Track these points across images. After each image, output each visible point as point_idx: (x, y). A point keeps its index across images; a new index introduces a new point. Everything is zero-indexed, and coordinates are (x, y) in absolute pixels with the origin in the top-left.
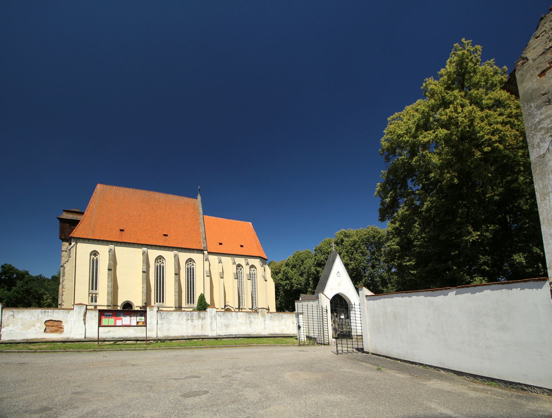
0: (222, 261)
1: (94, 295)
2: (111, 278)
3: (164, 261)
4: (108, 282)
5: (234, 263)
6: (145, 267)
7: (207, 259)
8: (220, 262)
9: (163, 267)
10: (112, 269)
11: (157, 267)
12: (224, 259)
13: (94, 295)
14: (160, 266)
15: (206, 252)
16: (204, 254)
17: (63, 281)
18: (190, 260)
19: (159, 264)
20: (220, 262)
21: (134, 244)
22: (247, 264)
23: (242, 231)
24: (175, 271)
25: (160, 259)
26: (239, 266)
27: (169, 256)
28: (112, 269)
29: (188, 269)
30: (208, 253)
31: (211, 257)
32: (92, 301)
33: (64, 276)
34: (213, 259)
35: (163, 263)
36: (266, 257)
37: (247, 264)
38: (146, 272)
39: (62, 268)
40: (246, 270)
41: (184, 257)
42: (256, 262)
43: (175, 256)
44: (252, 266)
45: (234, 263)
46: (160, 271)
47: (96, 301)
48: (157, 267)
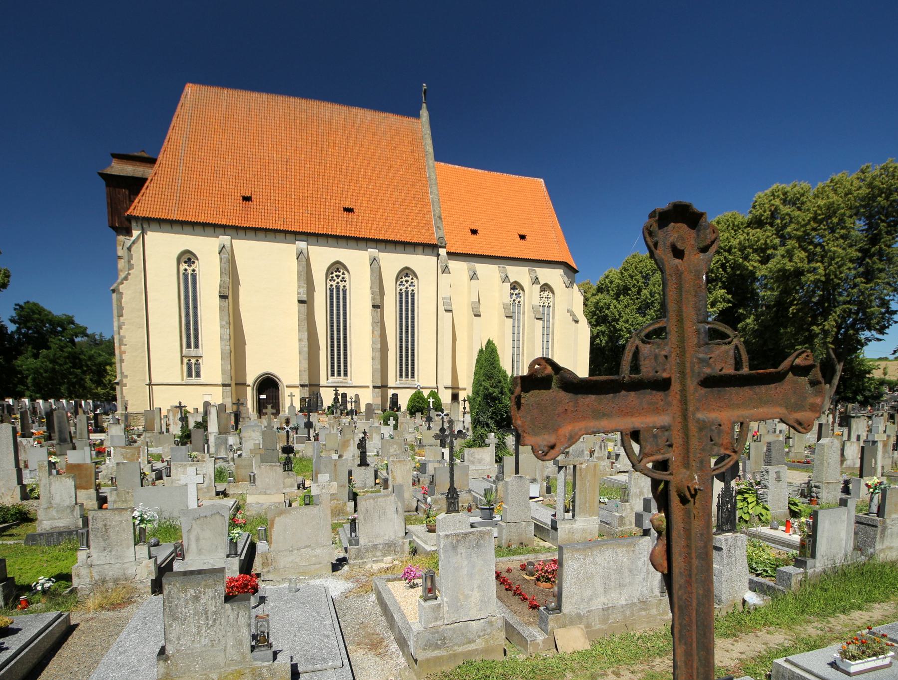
0: (478, 273)
1: (193, 361)
2: (227, 319)
3: (346, 276)
4: (221, 327)
5: (506, 279)
6: (303, 290)
7: (446, 270)
8: (474, 276)
9: (344, 292)
10: (229, 295)
11: (331, 291)
12: (482, 268)
13: (193, 361)
14: (338, 288)
15: (442, 252)
16: (438, 255)
17: (120, 328)
18: (406, 273)
19: (334, 284)
20: (474, 276)
21: (266, 231)
22: (536, 281)
23: (519, 201)
24: (373, 299)
25: (338, 270)
26: (515, 286)
27: (357, 260)
28: (229, 295)
29: (401, 294)
30: (448, 253)
31: (453, 265)
32: (190, 375)
33: (120, 315)
34: (459, 268)
35: (343, 280)
36: (574, 266)
37: (536, 281)
38: (306, 302)
39: (114, 296)
40: (532, 296)
41: (392, 262)
42: (554, 277)
43: (374, 260)
44: (546, 288)
45: (506, 279)
46: (338, 300)
47: (198, 375)
48: (331, 291)
